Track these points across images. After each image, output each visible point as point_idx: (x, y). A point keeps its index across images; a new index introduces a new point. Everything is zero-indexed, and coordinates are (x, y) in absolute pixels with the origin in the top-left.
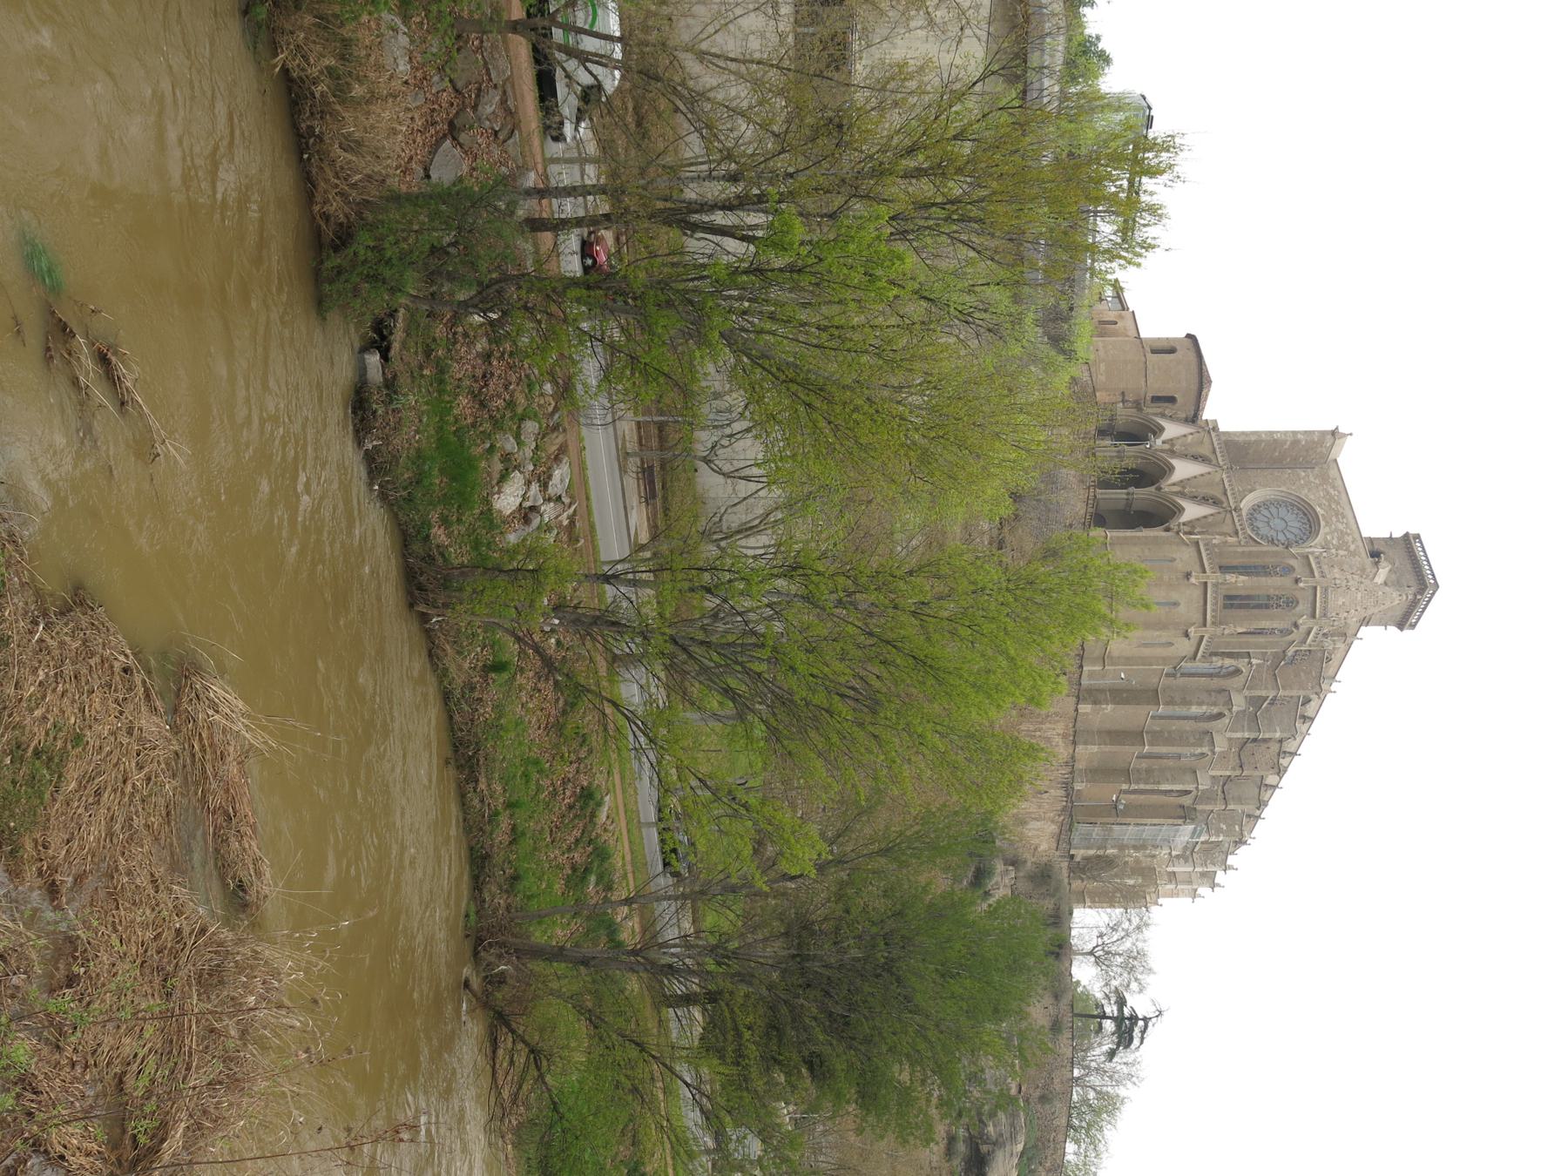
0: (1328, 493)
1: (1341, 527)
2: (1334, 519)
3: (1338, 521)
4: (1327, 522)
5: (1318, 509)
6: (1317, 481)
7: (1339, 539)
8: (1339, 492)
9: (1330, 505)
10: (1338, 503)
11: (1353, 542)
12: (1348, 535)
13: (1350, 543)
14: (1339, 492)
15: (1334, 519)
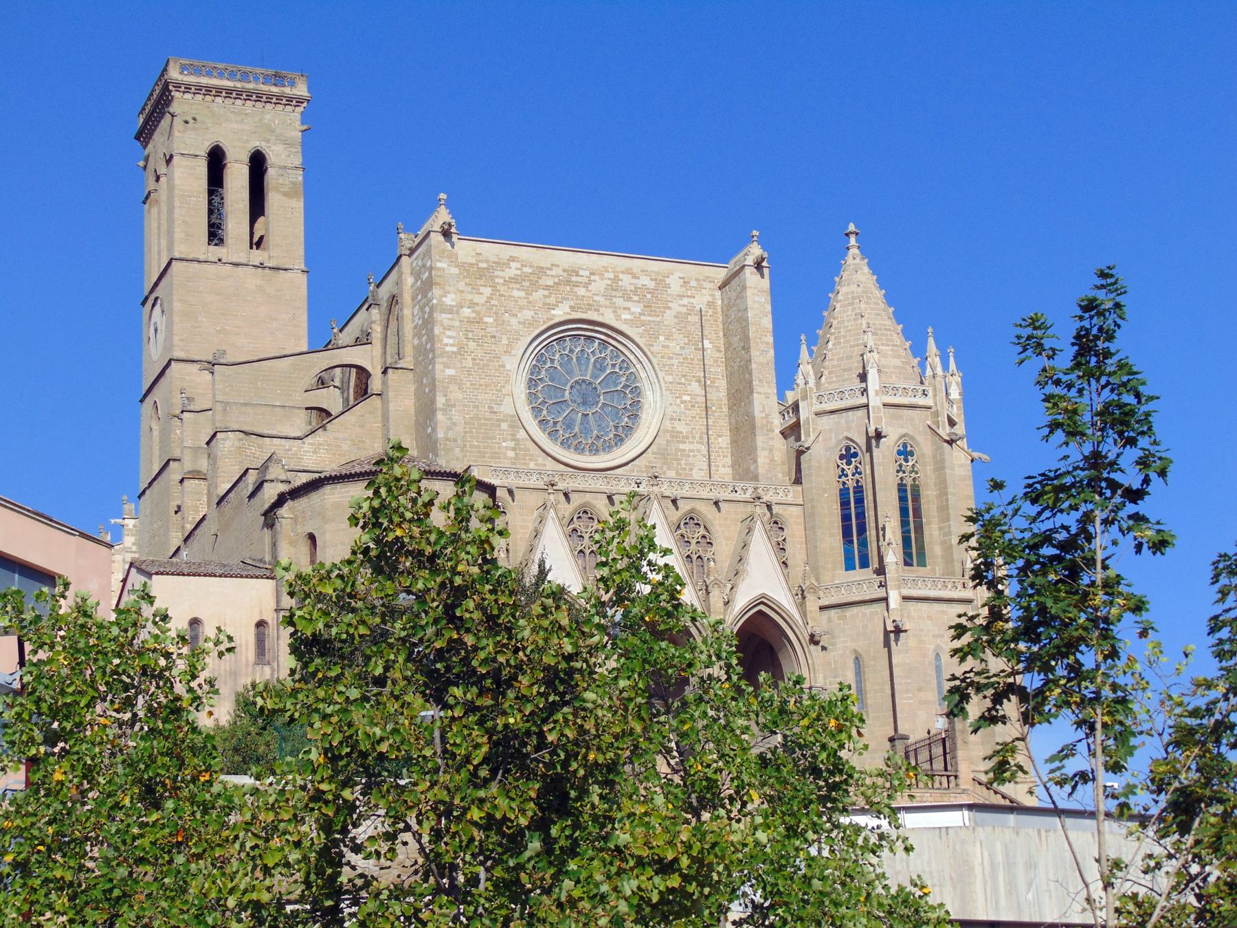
0: (514, 280)
1: (599, 285)
2: (581, 291)
3: (586, 285)
4: (590, 307)
5: (560, 313)
6: (487, 291)
7: (629, 299)
8: (513, 259)
9: (547, 288)
10: (541, 271)
11: (635, 277)
12: (616, 279)
13: (639, 283)
14: (513, 259)
15: (581, 291)
